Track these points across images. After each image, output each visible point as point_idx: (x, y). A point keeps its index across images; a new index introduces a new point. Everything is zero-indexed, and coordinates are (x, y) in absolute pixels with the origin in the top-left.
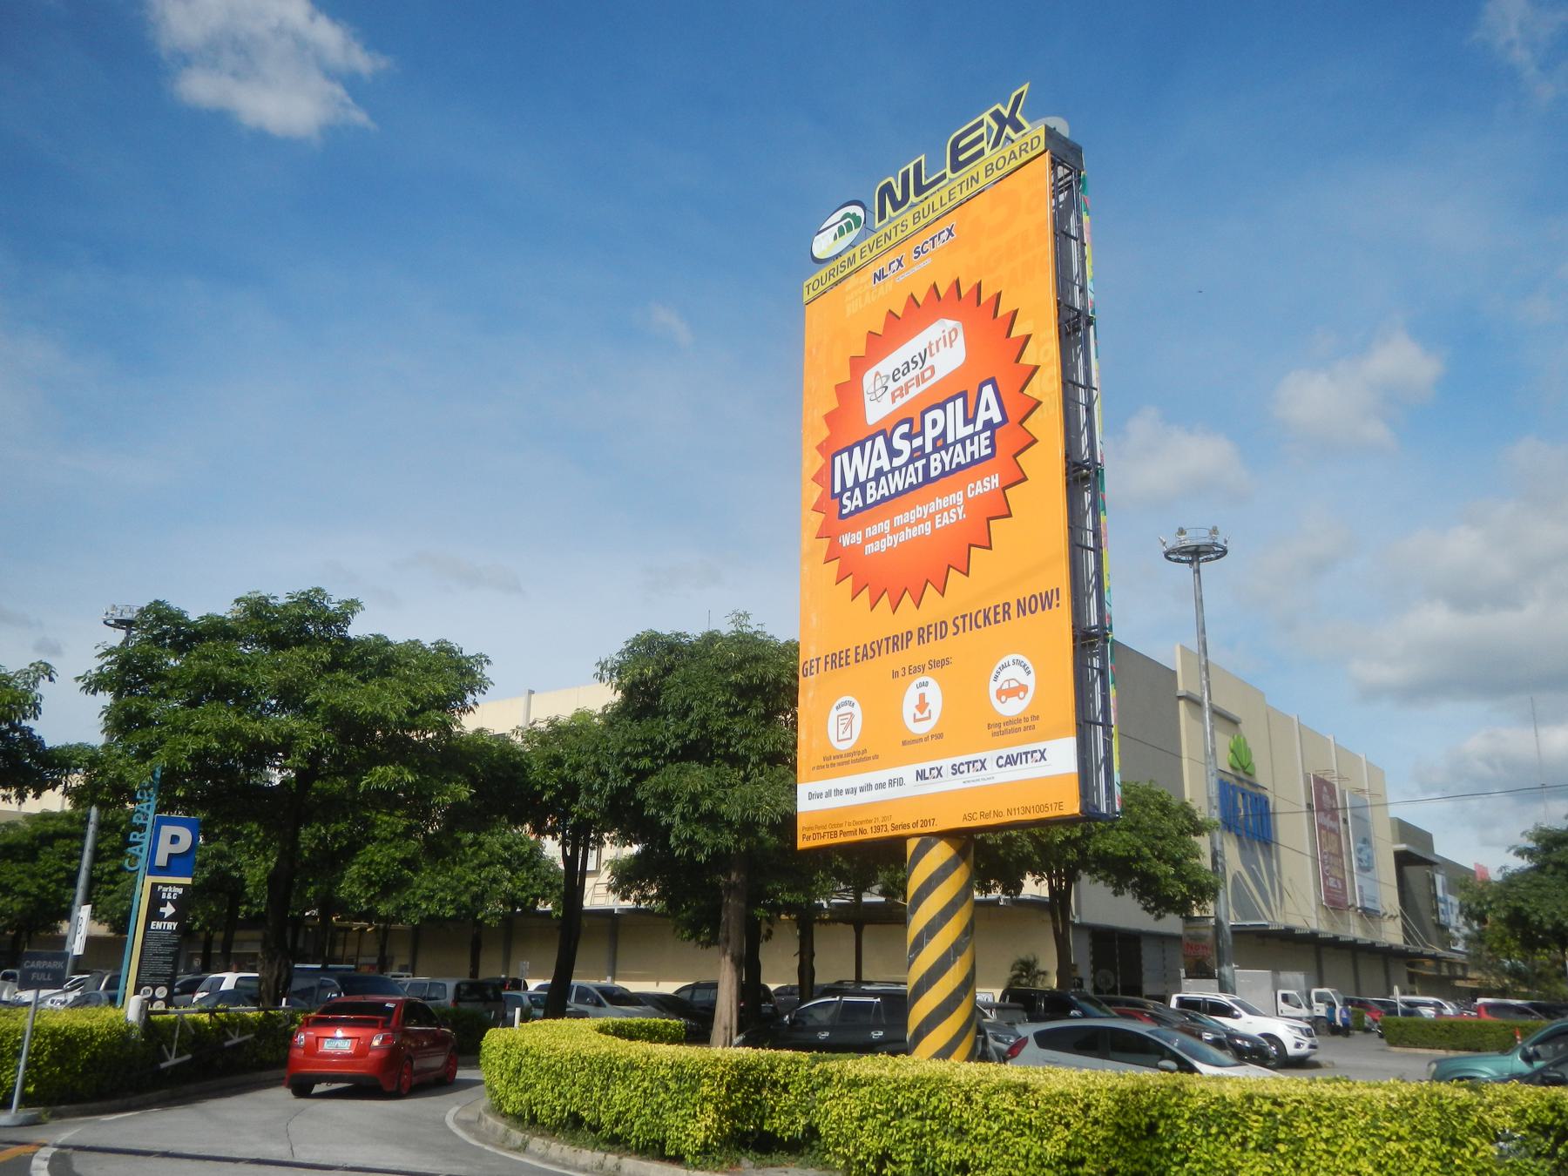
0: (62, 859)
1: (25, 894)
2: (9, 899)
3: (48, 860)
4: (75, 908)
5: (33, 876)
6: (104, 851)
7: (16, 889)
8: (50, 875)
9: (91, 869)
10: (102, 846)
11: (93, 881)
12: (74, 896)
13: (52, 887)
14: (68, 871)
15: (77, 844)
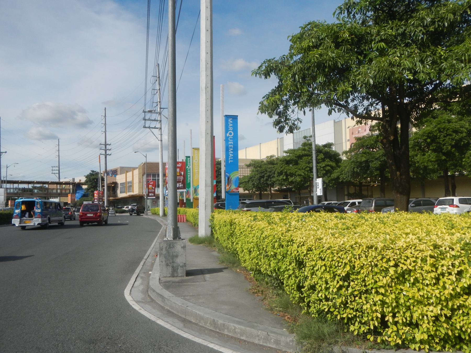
0: (306, 163)
1: (300, 175)
2: (293, 178)
3: (302, 163)
4: (314, 179)
5: (299, 169)
6: (319, 160)
7: (297, 174)
8: (305, 169)
9: (317, 166)
10: (319, 158)
11: (317, 170)
12: (313, 175)
13: (307, 173)
14: (309, 167)
15: (310, 158)
